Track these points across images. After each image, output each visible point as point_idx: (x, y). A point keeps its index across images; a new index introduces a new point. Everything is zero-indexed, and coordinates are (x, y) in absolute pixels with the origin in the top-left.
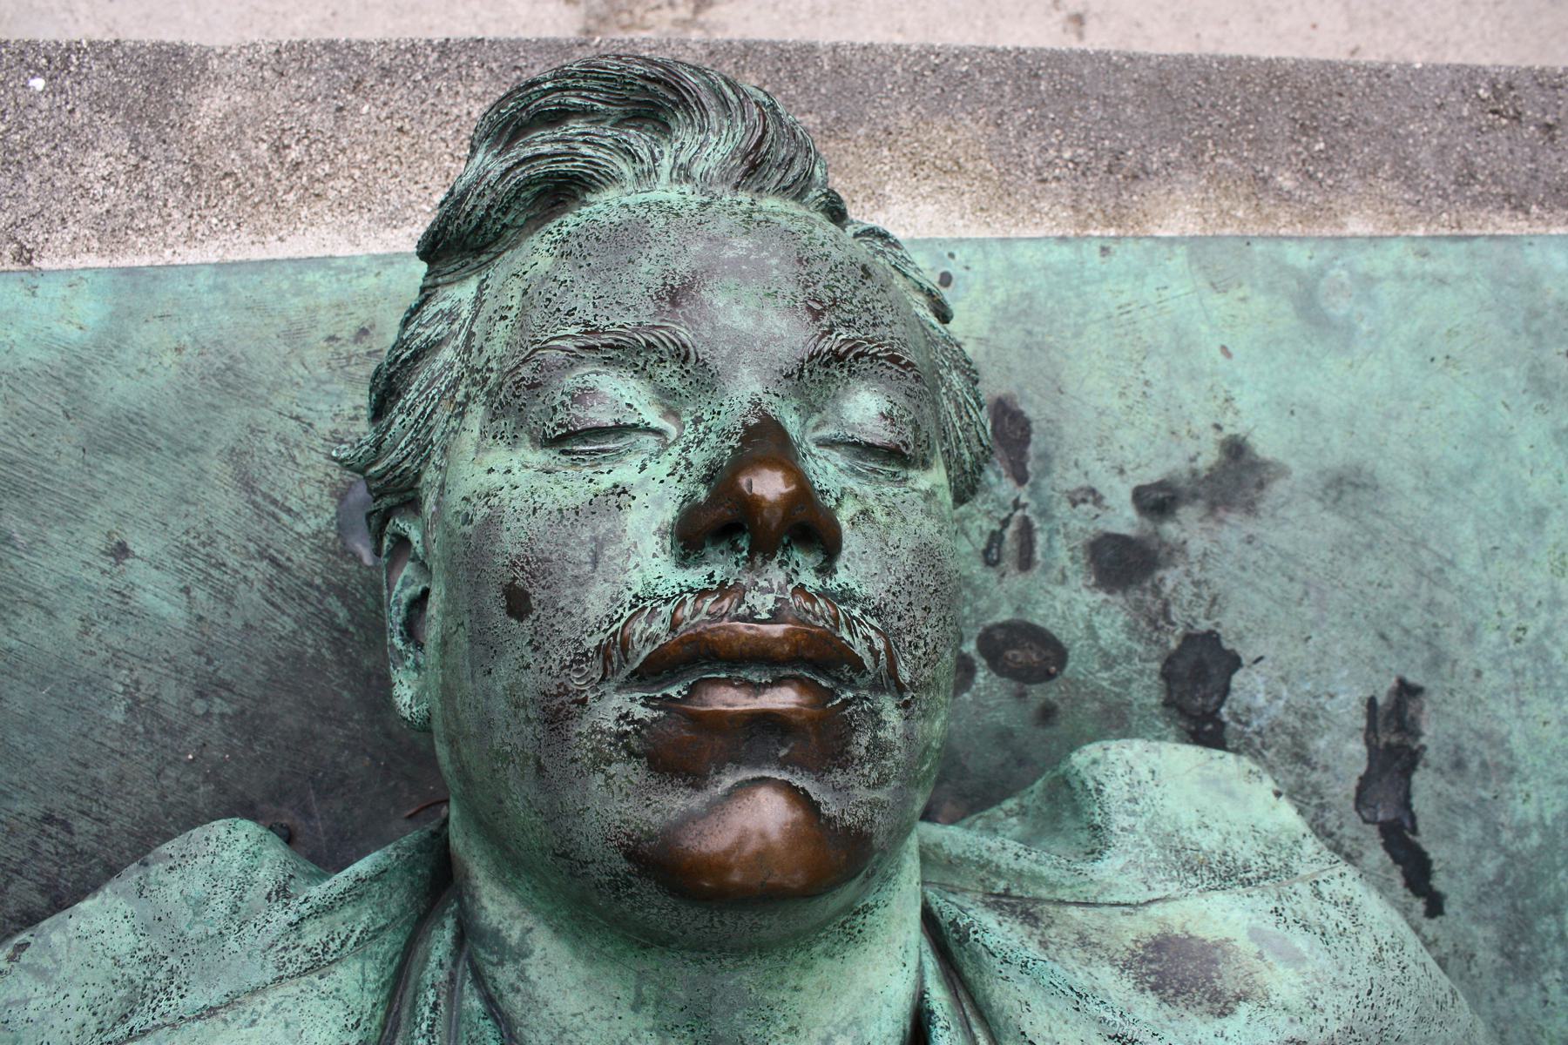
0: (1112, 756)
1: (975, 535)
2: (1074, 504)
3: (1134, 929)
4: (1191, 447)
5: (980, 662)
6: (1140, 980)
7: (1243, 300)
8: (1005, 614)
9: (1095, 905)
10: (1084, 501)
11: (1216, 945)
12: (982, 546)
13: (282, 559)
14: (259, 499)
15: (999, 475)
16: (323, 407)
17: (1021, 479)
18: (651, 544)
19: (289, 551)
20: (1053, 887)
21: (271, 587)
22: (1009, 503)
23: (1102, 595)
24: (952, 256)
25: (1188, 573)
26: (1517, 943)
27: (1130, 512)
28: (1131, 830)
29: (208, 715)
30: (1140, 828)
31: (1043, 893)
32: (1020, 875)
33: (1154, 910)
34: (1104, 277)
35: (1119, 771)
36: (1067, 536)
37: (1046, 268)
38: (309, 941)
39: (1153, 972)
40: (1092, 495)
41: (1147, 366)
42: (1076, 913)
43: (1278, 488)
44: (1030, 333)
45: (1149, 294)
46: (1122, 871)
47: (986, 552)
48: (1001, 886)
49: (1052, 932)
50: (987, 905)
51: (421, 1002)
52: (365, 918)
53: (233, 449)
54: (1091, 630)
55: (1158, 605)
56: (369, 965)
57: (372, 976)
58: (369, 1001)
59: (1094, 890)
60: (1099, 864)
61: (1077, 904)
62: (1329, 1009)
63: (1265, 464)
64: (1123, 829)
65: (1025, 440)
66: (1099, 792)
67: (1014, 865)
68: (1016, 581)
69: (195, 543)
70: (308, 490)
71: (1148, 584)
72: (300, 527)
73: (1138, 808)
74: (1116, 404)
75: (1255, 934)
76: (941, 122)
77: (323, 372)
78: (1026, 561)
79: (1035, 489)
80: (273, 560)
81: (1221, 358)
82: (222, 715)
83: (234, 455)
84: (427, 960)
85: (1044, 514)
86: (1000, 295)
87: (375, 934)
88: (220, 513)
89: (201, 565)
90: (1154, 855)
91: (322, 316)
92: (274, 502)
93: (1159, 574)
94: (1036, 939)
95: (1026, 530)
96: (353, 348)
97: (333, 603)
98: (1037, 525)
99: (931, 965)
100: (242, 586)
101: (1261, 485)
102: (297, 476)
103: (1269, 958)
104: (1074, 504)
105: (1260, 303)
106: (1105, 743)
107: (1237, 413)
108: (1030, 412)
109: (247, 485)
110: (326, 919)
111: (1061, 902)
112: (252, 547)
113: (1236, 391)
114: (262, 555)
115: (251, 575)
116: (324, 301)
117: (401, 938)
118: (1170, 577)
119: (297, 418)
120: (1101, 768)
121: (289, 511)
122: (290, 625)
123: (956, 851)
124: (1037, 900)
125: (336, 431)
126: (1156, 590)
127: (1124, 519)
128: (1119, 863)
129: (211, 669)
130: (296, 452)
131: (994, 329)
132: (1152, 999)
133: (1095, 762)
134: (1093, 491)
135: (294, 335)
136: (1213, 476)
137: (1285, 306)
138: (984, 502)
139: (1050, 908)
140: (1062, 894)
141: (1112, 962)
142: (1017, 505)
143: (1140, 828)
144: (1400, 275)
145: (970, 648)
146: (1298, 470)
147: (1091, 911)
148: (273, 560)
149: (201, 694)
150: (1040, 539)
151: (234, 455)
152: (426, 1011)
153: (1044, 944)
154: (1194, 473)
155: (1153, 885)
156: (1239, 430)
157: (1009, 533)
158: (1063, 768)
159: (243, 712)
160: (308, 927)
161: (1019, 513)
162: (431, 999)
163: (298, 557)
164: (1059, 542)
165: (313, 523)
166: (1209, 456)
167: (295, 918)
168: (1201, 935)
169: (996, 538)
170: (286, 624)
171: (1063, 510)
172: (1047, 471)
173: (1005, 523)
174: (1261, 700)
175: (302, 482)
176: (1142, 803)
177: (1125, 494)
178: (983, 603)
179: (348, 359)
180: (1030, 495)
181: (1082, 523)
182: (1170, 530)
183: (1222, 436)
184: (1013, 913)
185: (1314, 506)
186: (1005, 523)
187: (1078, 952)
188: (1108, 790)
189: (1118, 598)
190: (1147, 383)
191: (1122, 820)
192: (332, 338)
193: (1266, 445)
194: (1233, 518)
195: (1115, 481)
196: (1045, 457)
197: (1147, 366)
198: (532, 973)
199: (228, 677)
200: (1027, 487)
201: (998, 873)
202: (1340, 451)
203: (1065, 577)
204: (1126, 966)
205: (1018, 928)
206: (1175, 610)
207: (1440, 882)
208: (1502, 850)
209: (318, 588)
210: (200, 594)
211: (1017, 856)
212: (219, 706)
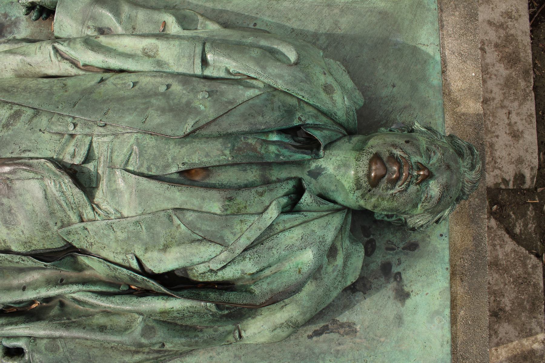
1: (393, 239)
2: (398, 260)
3: (338, 245)
4: (408, 285)
5: (368, 239)
7: (438, 299)
8: (378, 244)
10: (398, 262)
11: (336, 258)
12: (391, 240)
15: (404, 244)
17: (403, 249)
18: (416, 159)
20: (344, 233)
22: (399, 246)
23: (380, 264)
24: (446, 237)
25: (383, 283)
26: (299, 357)
27: (396, 271)
30: (353, 250)
31: (343, 232)
32: (346, 229)
33: (341, 249)
34: (442, 268)
36: (392, 258)
37: (444, 256)
40: (400, 263)
41: (425, 277)
43: (399, 305)
44: (431, 252)
45: (439, 278)
47: (390, 241)
54: (373, 262)
55: (377, 277)
59: (344, 240)
62: (325, 276)
63: (404, 302)
65: (410, 250)
68: (383, 247)
70: (404, 118)
71: (382, 275)
72: (398, 116)
74: (417, 269)
75: (337, 265)
76: (472, 239)
77: (425, 121)
78: (387, 249)
79: (401, 252)
80: (392, 111)
81: (426, 293)
83: (410, 105)
85: (396, 253)
86: (439, 246)
91: (434, 121)
93: (384, 277)
95: (393, 249)
97: (385, 121)
101: (400, 300)
103: (334, 267)
104: (398, 260)
105: (437, 302)
107: (415, 296)
108: (416, 251)
109: (405, 108)
113: (419, 296)
116: (437, 122)
118: (383, 279)
121: (401, 114)
126: (380, 276)
127: (395, 270)
131: (432, 244)
134: (400, 264)
135: (431, 116)
136: (402, 290)
137: (436, 308)
140: (343, 235)
142: (398, 248)
143: (353, 250)
144: (443, 336)
145: (372, 237)
146: (403, 309)
148: (392, 111)
150: (392, 252)
151: (410, 105)
154: (403, 286)
156: (412, 296)
157: (393, 246)
160: (352, 112)
163: (393, 116)
164: (391, 256)
166: (406, 289)
169: (392, 243)
170: (381, 113)
171: (397, 257)
172: (404, 254)
174: (357, 298)
177: (399, 270)
178: (380, 240)
181: (394, 261)
182: (392, 280)
183: (410, 292)
185: (395, 312)
190: (421, 276)
192: (430, 122)
194: (394, 293)
195: (402, 268)
196: (407, 254)
197: (425, 277)
198: (347, 143)
202: (407, 319)
203: (384, 257)
206: (375, 280)
207: (315, 339)
208: (320, 354)
210: (386, 99)
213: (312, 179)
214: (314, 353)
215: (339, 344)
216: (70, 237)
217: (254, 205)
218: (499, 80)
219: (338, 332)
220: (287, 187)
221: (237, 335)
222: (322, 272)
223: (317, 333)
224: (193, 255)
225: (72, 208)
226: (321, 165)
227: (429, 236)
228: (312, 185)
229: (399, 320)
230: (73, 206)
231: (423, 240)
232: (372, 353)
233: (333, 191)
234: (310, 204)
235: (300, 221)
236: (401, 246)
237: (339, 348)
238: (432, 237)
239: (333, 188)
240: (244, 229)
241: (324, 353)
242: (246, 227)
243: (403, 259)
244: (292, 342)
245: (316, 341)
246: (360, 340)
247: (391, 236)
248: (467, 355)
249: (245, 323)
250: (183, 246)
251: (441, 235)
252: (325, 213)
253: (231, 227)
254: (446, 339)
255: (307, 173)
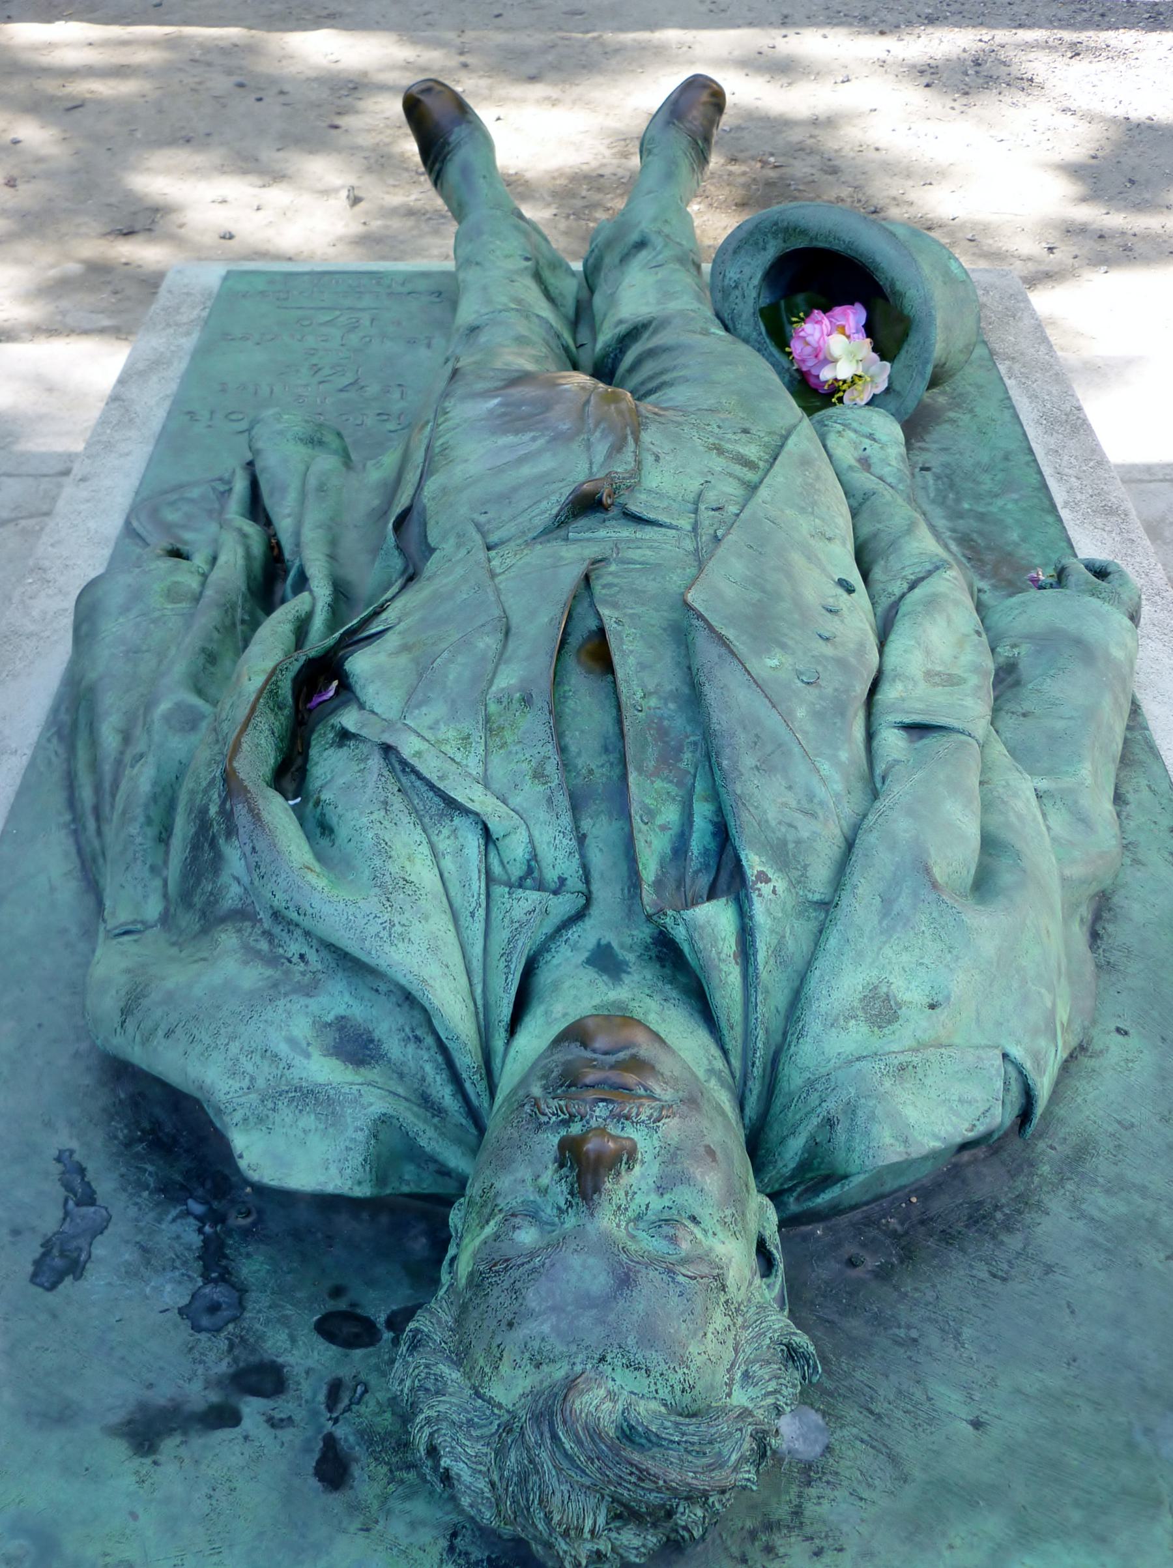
0: (349, 1183)
1: (372, 1403)
6: (378, 1047)
9: (391, 1092)
13: (865, 1413)
14: (884, 1450)
15: (346, 1440)
16: (844, 1506)
17: (330, 1441)
19: (861, 1417)
20: (409, 1109)
21: (872, 1398)
28: (357, 1129)
29: (909, 1327)
31: (415, 1109)
33: (360, 1080)
35: (349, 1171)
38: (816, 1095)
39: (370, 1050)
42: (401, 1091)
44: (303, 1536)
46: (371, 1104)
47: (366, 1391)
48: (436, 1120)
49: (416, 1086)
50: (446, 1112)
51: (760, 1070)
52: (790, 1115)
53: (905, 1482)
56: (786, 1090)
57: (785, 1084)
58: (786, 1071)
60: (383, 1111)
61: (399, 1096)
64: (362, 1130)
66: (365, 1160)
67: (427, 1128)
69: (926, 1426)
70: (850, 1453)
72: (855, 1431)
73: (347, 1143)
77: (845, 1528)
80: (872, 1412)
82: (899, 1327)
84: (759, 1098)
87: (786, 1107)
88: (910, 1443)
89: (920, 1413)
90: (349, 1111)
92: (873, 1447)
94: (426, 1084)
96: (824, 1544)
98: (323, 1407)
99: (497, 1062)
100: (892, 1398)
102: (859, 1463)
106: (351, 1194)
108: (314, 1482)
109: (894, 1459)
110: (808, 1109)
111: (406, 1099)
112: (886, 1421)
114: (879, 1417)
115: (886, 1405)
117: (772, 1112)
119: (861, 1499)
120: (358, 1176)
121: (862, 1441)
122: (858, 1374)
123: (454, 1148)
124: (419, 1106)
125: (833, 1490)
128: (372, 1109)
129: (909, 1353)
130: (860, 1477)
132: (376, 1035)
133: (360, 1183)
138: (362, 1423)
139: (413, 1099)
140: (407, 1104)
141: (389, 1061)
147: (393, 1089)
148: (872, 1412)
149: (915, 1340)
152: (757, 1063)
153: (423, 1079)
155: (356, 1093)
158: (376, 1191)
159: (885, 1329)
161: (335, 1415)
162: (755, 1070)
165: (845, 1433)
167: (824, 1104)
168: (338, 1062)
173: (348, 1409)
175: (855, 1459)
176: (343, 1148)
179: (827, 1536)
180: (323, 1426)
184: (433, 1103)
186: (348, 1409)
187: (406, 1070)
188: (361, 1159)
191: (361, 1137)
192: (841, 1550)
196: (307, 1450)
199: (896, 1348)
200: (325, 1432)
201: (436, 1128)
204: (382, 1056)
205: (434, 1093)
209: (839, 1395)
211: (424, 1132)
212: (902, 1333)
213: (587, 954)
220: (561, 854)
226: (629, 973)
227: (368, 1530)
228: (569, 954)
231: (355, 1508)
235: (458, 901)
236: (342, 1431)
243: (287, 1434)
252: (479, 990)
255: (603, 942)
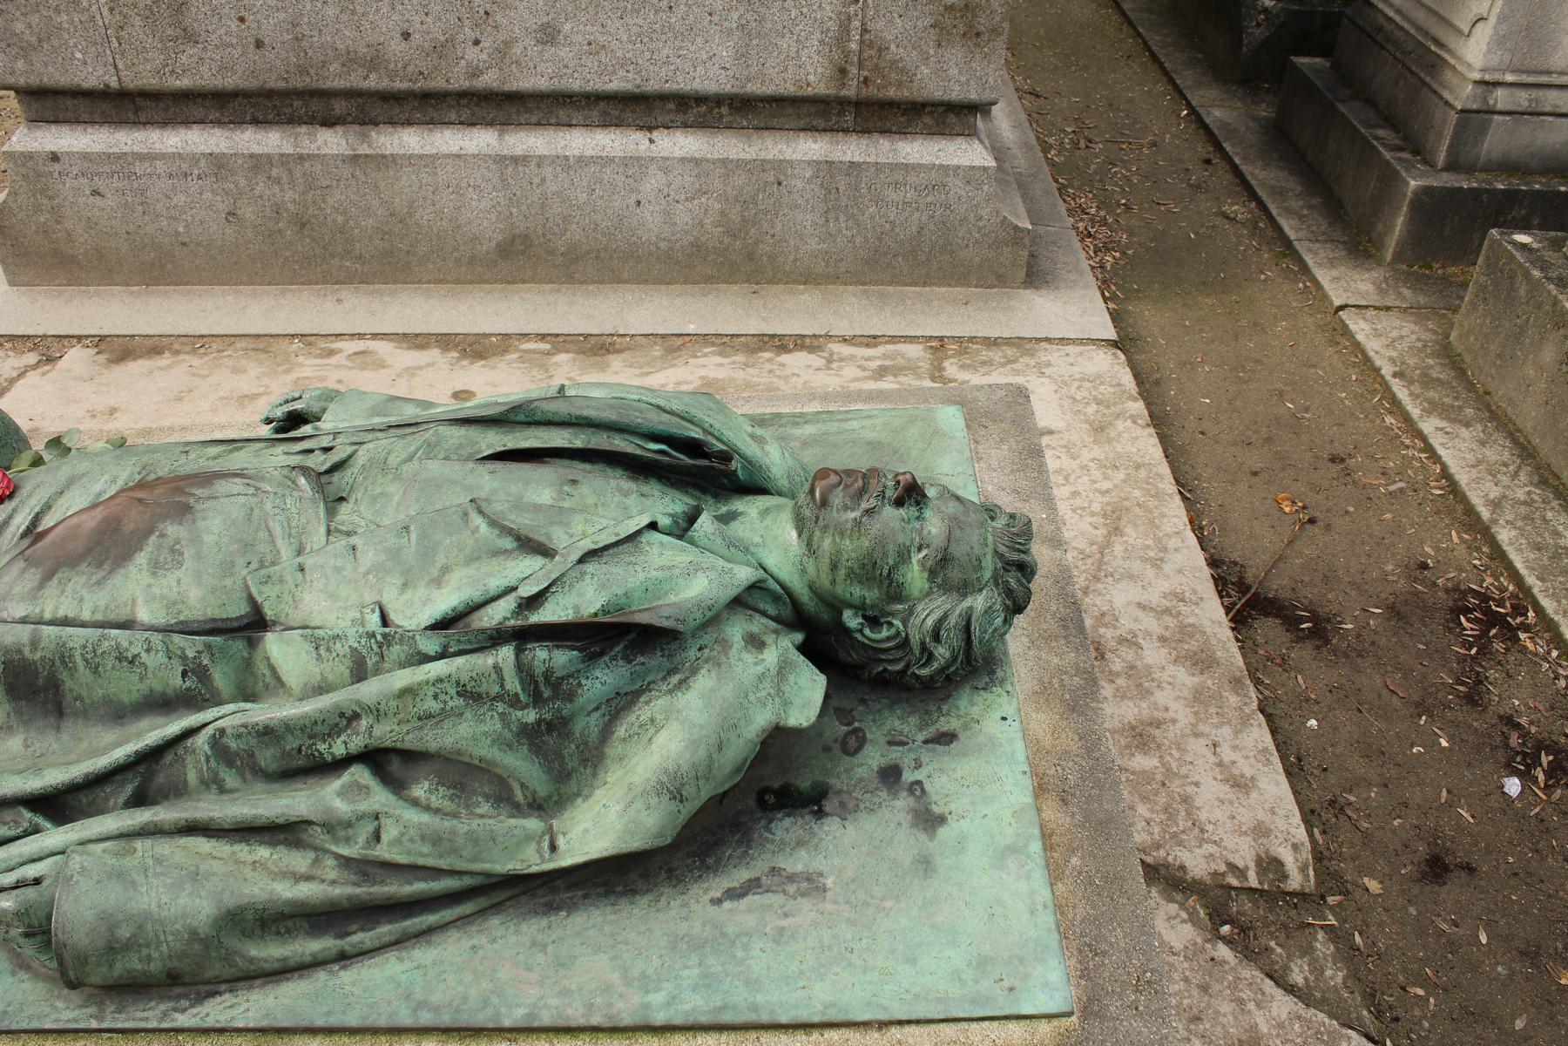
4: (942, 802)
5: (850, 728)
8: (869, 736)
17: (926, 742)
26: (688, 943)
27: (911, 779)
34: (1013, 772)
37: (1014, 752)
40: (918, 765)
43: (923, 837)
45: (1007, 788)
63: (935, 831)
74: (959, 775)
76: (1076, 738)
78: (890, 743)
105: (1010, 831)
108: (952, 746)
118: (884, 794)
127: (908, 776)
136: (928, 811)
137: (1009, 841)
145: (856, 724)
146: (932, 846)
150: (900, 748)
154: (930, 804)
166: (936, 810)
172: (928, 751)
174: (826, 828)
178: (874, 729)
181: (907, 762)
182: (905, 794)
185: (916, 852)
189: (875, 774)
193: (943, 832)
194: (909, 817)
196: (934, 750)
207: (727, 905)
208: (738, 936)
214: (723, 935)
215: (786, 915)
216: (265, 589)
217: (613, 505)
218: (1181, 691)
219: (784, 892)
220: (671, 506)
221: (546, 845)
222: (731, 654)
223: (734, 894)
224: (490, 575)
225: (290, 535)
229: (926, 864)
230: (293, 532)
232: (866, 933)
233: (757, 545)
234: (712, 537)
236: (921, 737)
237: (784, 923)
238: (984, 723)
239: (757, 539)
240: (590, 532)
241: (749, 935)
242: (593, 530)
243: (924, 759)
244: (672, 913)
245: (730, 910)
246: (834, 907)
247: (897, 723)
248: (1104, 947)
249: (567, 814)
250: (477, 564)
251: (1004, 719)
253: (567, 525)
254: (1039, 899)
